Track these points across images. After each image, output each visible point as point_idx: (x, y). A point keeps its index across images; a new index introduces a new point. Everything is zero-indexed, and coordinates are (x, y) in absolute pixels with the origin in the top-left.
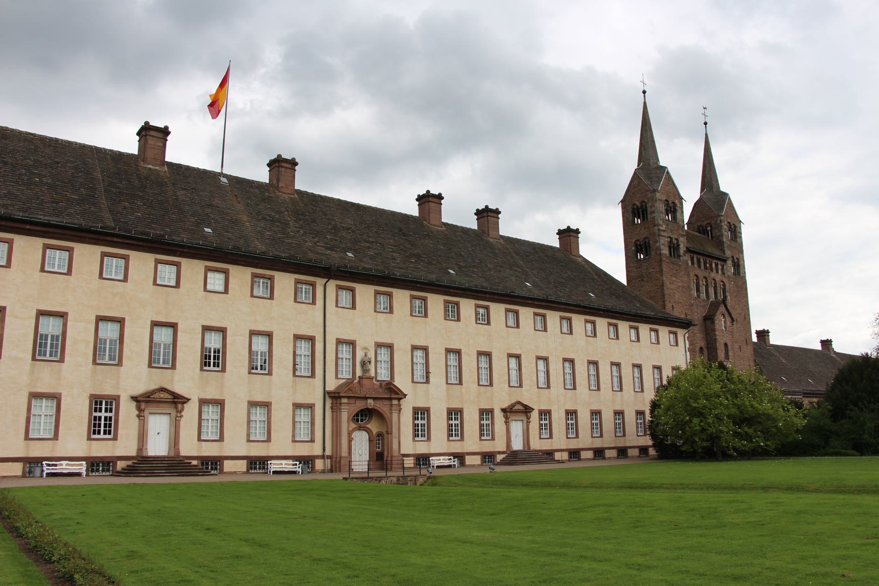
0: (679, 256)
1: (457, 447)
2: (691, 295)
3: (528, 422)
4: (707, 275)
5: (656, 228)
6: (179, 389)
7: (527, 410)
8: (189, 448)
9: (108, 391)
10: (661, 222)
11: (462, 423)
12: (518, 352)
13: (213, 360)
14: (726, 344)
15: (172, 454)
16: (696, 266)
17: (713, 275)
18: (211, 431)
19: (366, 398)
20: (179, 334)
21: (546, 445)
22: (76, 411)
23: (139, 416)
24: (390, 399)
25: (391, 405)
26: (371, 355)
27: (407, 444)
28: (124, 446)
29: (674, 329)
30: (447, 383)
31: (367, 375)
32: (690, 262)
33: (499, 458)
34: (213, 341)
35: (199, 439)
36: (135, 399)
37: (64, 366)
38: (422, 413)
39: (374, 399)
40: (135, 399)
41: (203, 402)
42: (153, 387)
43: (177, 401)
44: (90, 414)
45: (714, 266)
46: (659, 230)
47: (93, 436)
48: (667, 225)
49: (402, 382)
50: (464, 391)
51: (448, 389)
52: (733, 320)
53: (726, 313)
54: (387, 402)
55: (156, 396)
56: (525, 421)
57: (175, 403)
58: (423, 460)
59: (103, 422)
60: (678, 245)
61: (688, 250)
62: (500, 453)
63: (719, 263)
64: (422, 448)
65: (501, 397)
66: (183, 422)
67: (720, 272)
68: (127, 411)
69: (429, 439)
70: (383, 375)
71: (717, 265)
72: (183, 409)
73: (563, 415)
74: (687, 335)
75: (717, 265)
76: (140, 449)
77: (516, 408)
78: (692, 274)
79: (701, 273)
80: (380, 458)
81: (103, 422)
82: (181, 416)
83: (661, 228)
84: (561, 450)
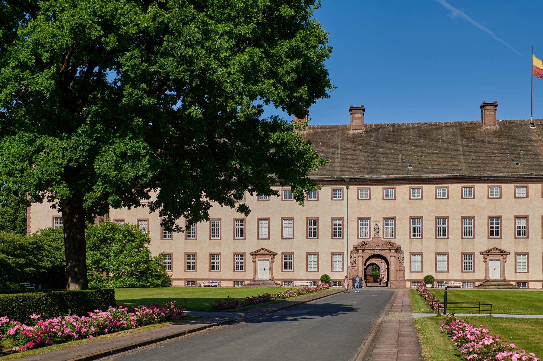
6: (504, 248)
8: (510, 276)
9: (469, 250)
13: (521, 232)
15: (502, 279)
18: (522, 267)
20: (503, 221)
22: (456, 259)
23: (484, 261)
28: (479, 275)
34: (521, 223)
35: (516, 272)
36: (482, 254)
37: (449, 240)
40: (482, 254)
41: (517, 254)
42: (491, 247)
43: (504, 254)
44: (462, 261)
47: (464, 271)
55: (493, 251)
57: (502, 255)
59: (468, 264)
66: (506, 264)
68: (479, 259)
72: (506, 258)
76: (486, 277)
81: (468, 264)
82: (506, 261)
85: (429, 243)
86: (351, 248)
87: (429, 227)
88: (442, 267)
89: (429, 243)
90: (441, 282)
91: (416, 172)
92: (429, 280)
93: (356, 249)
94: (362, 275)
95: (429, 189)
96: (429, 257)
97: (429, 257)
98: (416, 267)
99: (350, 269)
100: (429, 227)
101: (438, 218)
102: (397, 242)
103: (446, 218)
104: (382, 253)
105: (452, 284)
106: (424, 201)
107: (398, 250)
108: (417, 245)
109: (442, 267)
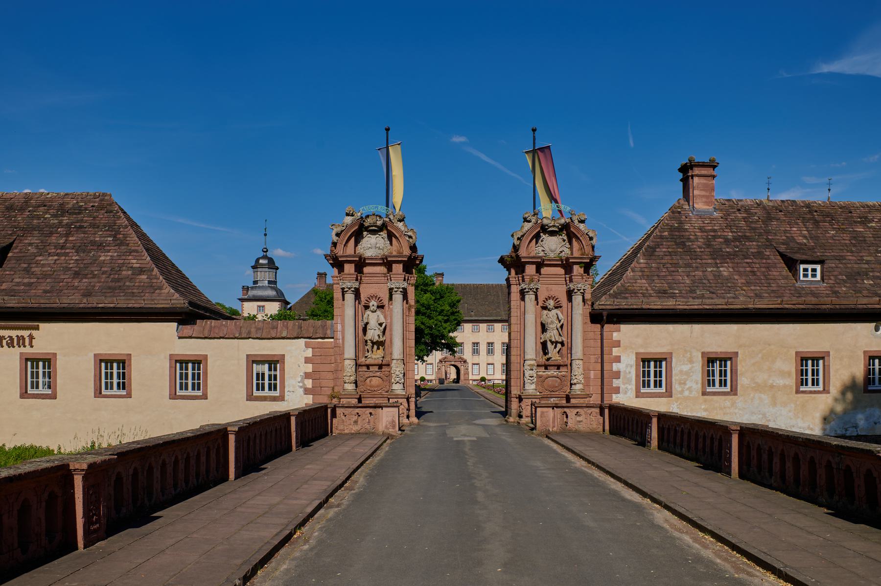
85: (483, 358)
86: (438, 361)
87: (483, 348)
88: (491, 372)
89: (483, 358)
90: (489, 380)
91: (476, 316)
92: (483, 379)
93: (441, 361)
94: (444, 377)
95: (483, 326)
96: (483, 366)
97: (483, 366)
98: (476, 372)
99: (437, 373)
100: (483, 348)
101: (489, 343)
102: (465, 357)
103: (492, 343)
104: (456, 364)
105: (496, 382)
106: (480, 333)
107: (465, 362)
108: (476, 359)
109: (491, 372)
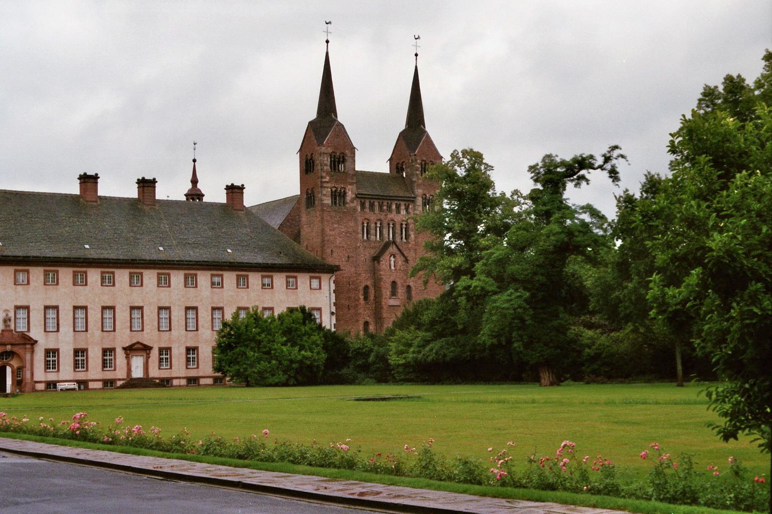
0: (345, 203)
1: (81, 376)
2: (356, 239)
3: (148, 357)
4: (382, 217)
5: (320, 180)
7: (146, 349)
10: (324, 174)
11: (87, 358)
12: (141, 305)
14: (394, 284)
16: (367, 210)
17: (390, 216)
19: (5, 345)
21: (165, 374)
24: (25, 344)
25: (25, 348)
26: (12, 314)
27: (40, 374)
29: (317, 275)
30: (74, 331)
31: (8, 328)
32: (359, 208)
33: (119, 383)
38: (52, 353)
39: (12, 345)
45: (394, 207)
46: (322, 182)
48: (331, 176)
49: (36, 333)
50: (89, 336)
51: (75, 335)
52: (407, 261)
53: (398, 252)
54: (21, 347)
56: (145, 357)
58: (51, 385)
60: (345, 193)
61: (358, 196)
62: (120, 380)
63: (402, 203)
64: (52, 377)
65: (123, 338)
67: (403, 212)
69: (58, 371)
70: (22, 328)
71: (398, 207)
73: (184, 351)
74: (333, 278)
75: (398, 207)
77: (136, 346)
78: (360, 219)
79: (373, 218)
80: (19, 383)
83: (324, 180)
84: (180, 378)
